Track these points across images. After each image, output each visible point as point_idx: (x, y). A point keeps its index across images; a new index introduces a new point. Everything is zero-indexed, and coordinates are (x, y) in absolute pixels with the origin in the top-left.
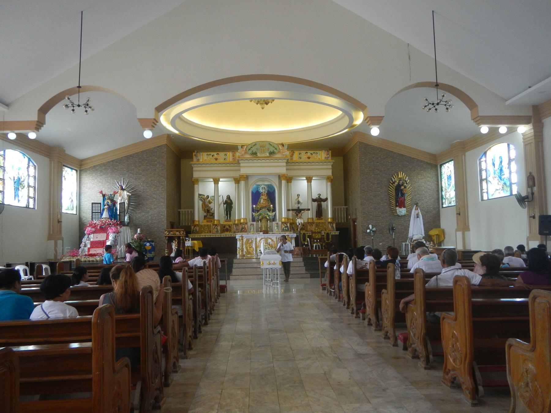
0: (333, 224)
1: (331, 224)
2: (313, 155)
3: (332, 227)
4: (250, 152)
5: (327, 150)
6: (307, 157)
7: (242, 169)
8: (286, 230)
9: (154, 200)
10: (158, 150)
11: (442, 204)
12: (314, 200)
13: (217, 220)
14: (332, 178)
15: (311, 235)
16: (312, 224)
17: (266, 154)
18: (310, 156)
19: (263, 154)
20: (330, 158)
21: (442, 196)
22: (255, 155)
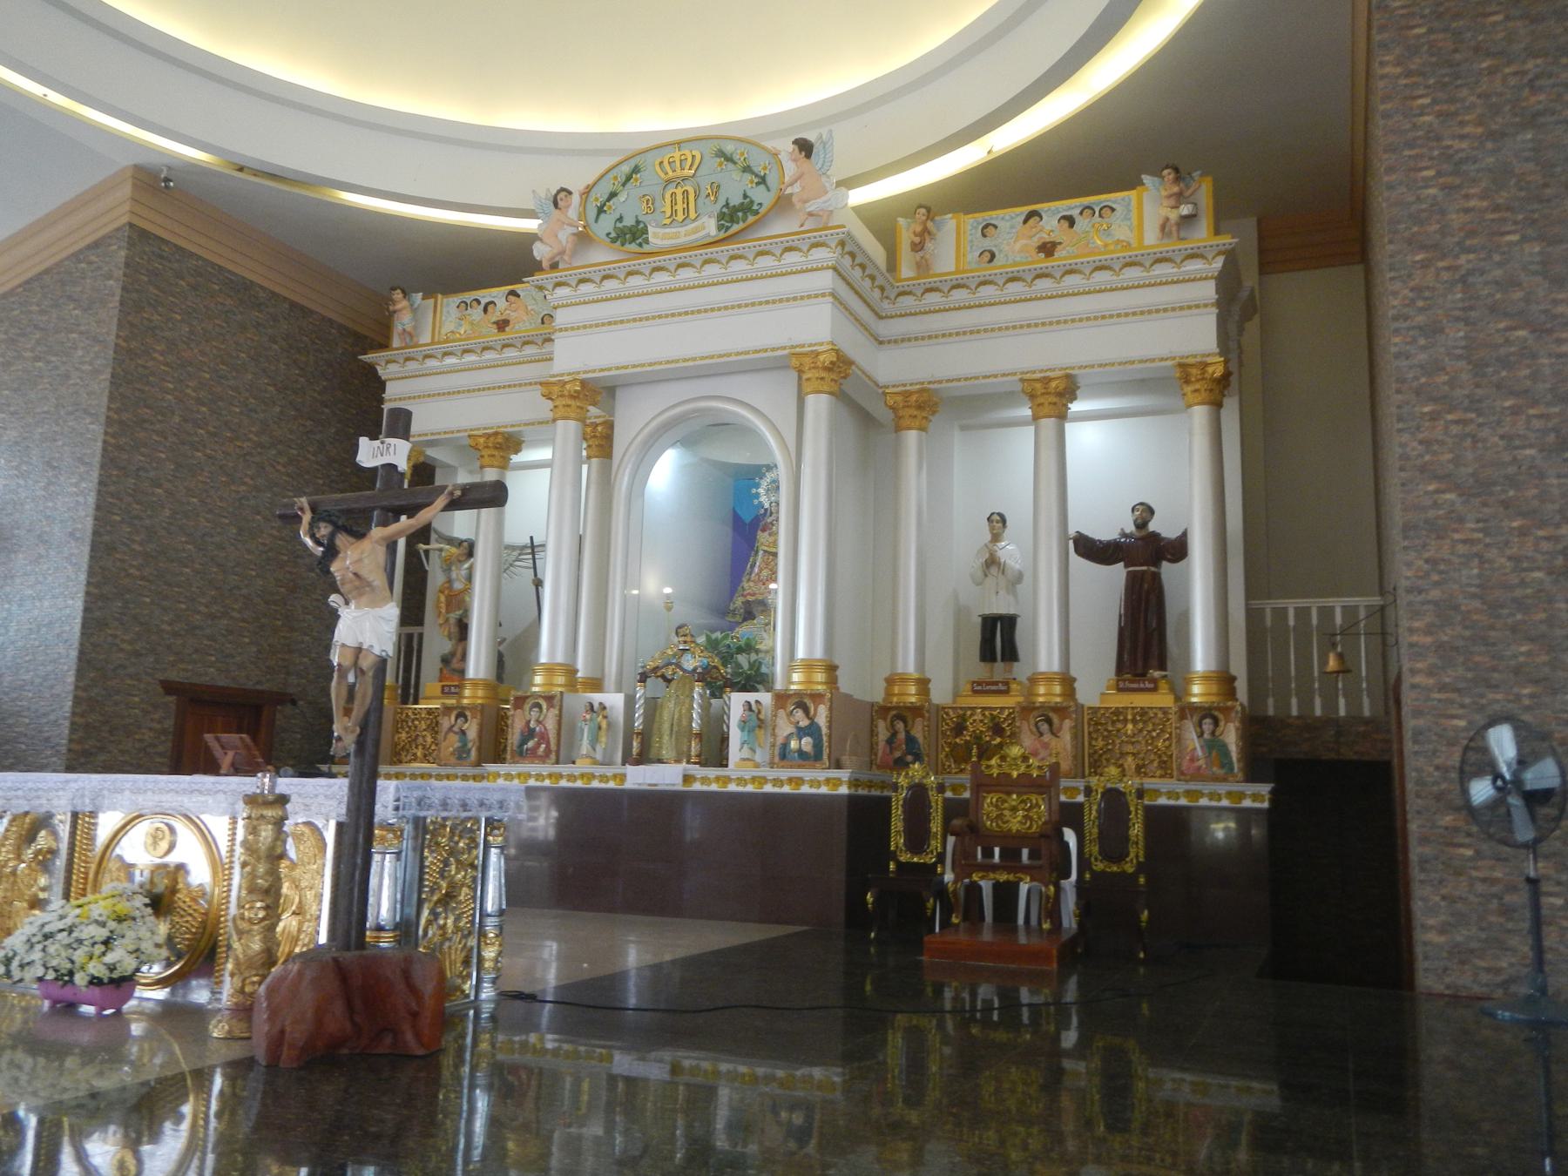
0: (1216, 722)
1: (1207, 725)
2: (1082, 223)
3: (1215, 746)
4: (607, 224)
5: (1177, 170)
6: (1036, 242)
8: (800, 752)
10: (90, 263)
12: (1090, 549)
13: (475, 683)
15: (966, 801)
16: (1049, 721)
18: (1054, 237)
22: (633, 240)
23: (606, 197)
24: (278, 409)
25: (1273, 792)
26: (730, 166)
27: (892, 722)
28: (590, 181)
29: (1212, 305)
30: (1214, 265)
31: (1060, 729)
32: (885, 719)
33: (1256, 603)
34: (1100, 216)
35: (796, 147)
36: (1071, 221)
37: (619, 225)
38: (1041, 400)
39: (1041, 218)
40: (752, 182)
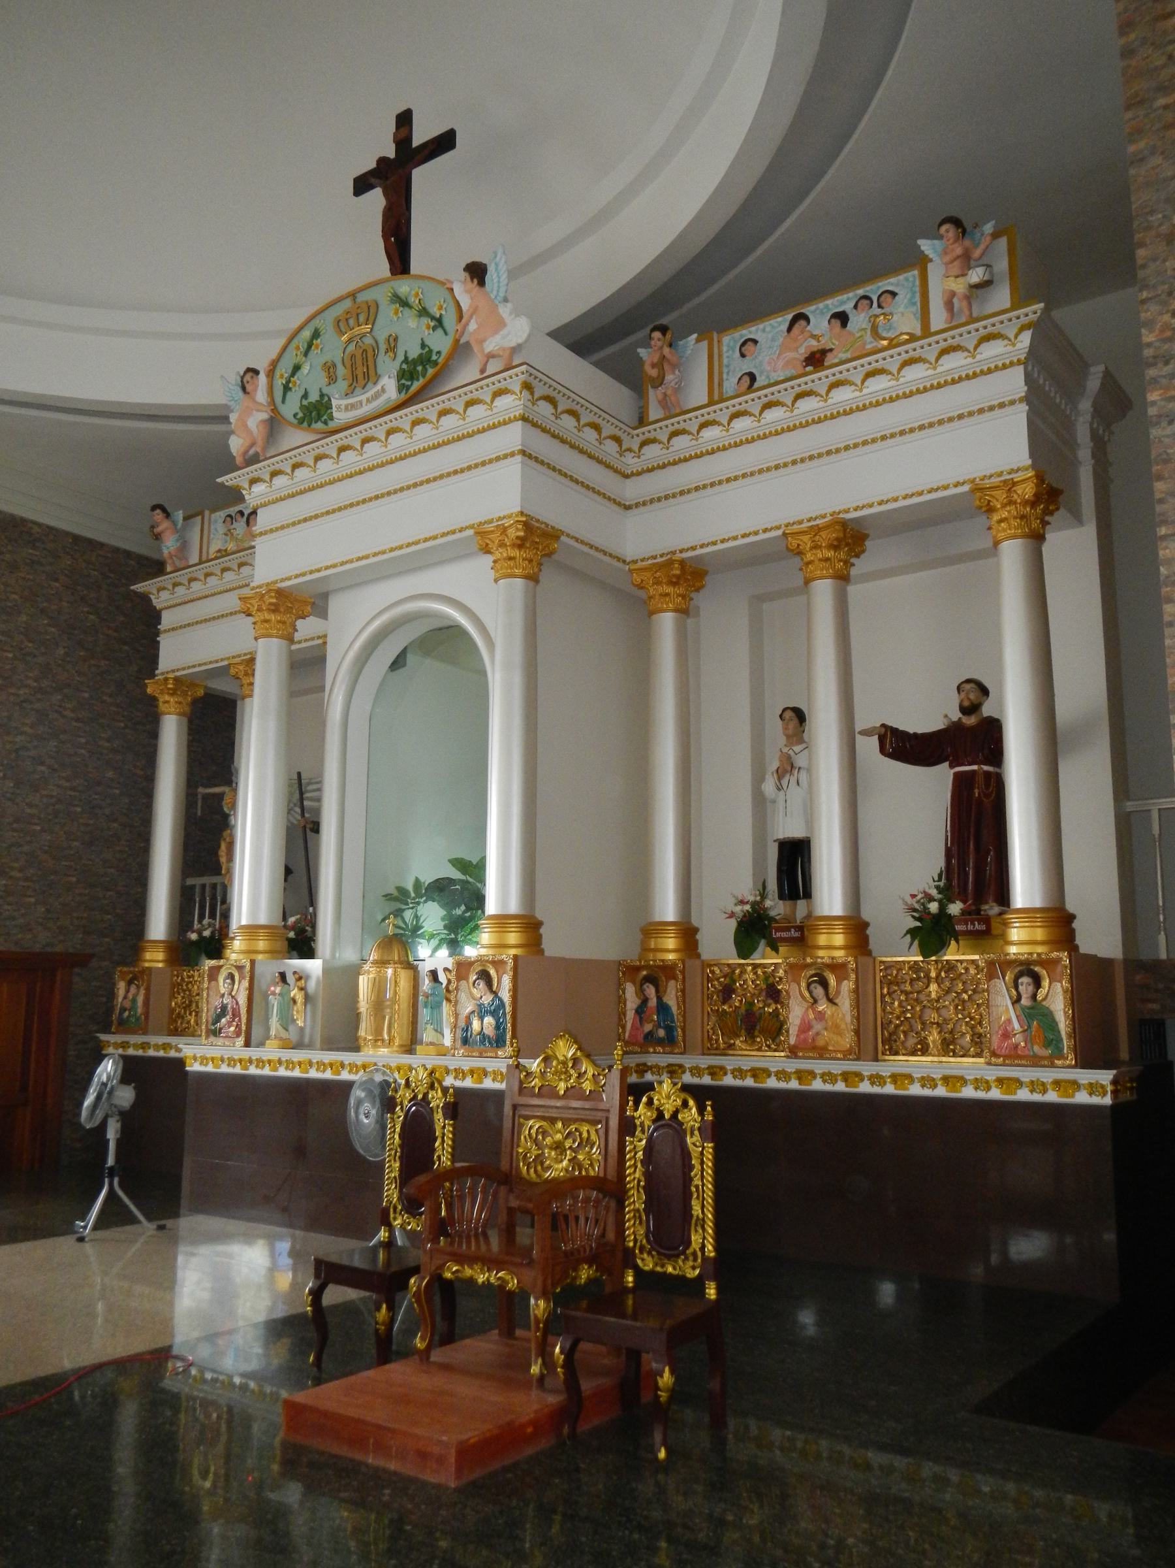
2: (859, 321)
3: (1037, 1014)
6: (803, 352)
7: (262, 546)
16: (824, 984)
17: (379, 387)
18: (825, 343)
19: (363, 398)
23: (290, 371)
24: (61, 651)
25: (1114, 1082)
26: (407, 311)
27: (641, 985)
28: (274, 356)
29: (1021, 400)
30: (1019, 346)
31: (838, 992)
32: (634, 982)
33: (1130, 806)
34: (880, 306)
35: (467, 274)
36: (842, 318)
37: (305, 403)
38: (809, 556)
39: (808, 321)
40: (428, 327)
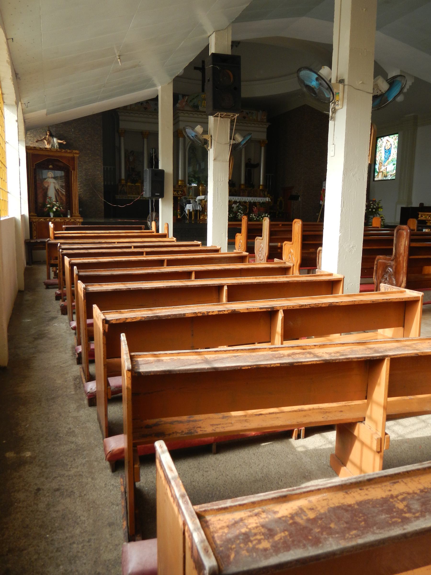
9: (89, 151)
11: (374, 177)
14: (267, 142)
20: (265, 120)
21: (375, 169)
36: (247, 113)
